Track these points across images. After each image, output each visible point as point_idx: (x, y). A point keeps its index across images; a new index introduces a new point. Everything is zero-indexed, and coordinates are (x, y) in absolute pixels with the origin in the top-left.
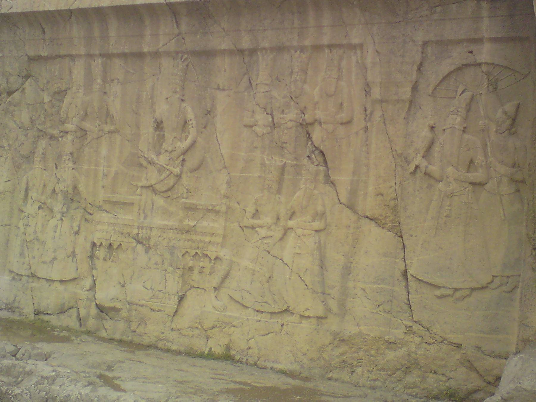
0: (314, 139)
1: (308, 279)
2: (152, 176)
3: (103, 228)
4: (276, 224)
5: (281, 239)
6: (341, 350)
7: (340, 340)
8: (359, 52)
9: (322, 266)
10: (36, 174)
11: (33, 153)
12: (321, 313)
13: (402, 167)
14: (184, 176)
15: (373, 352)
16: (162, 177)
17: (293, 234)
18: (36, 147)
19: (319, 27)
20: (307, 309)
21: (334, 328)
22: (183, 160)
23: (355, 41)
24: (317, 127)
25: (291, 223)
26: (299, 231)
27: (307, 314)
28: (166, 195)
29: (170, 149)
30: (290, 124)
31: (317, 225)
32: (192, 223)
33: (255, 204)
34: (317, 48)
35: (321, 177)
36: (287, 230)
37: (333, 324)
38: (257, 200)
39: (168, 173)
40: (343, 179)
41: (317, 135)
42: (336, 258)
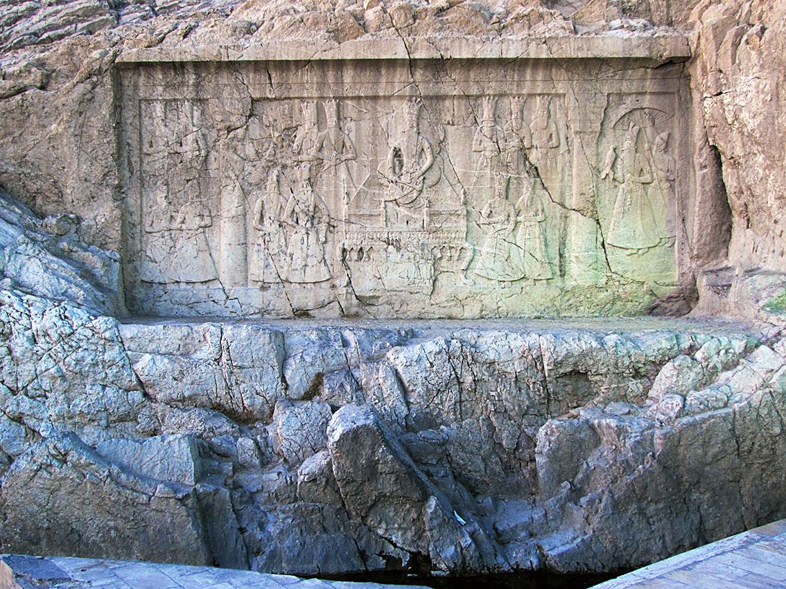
0: (530, 159)
1: (538, 255)
2: (396, 193)
3: (349, 237)
4: (508, 220)
5: (513, 230)
6: (566, 298)
7: (563, 291)
8: (562, 99)
9: (546, 245)
10: (269, 196)
11: (264, 181)
12: (550, 277)
13: (597, 175)
14: (424, 190)
15: (588, 296)
16: (405, 193)
17: (522, 226)
18: (267, 176)
19: (534, 81)
20: (539, 275)
21: (560, 284)
22: (424, 178)
23: (561, 92)
24: (534, 151)
25: (519, 219)
26: (527, 224)
27: (539, 278)
28: (408, 206)
29: (412, 171)
30: (513, 149)
31: (540, 218)
32: (438, 226)
33: (490, 206)
34: (531, 95)
35: (539, 186)
36: (517, 223)
37: (558, 281)
38: (490, 204)
39: (411, 189)
40: (555, 186)
41: (534, 156)
42: (554, 236)
